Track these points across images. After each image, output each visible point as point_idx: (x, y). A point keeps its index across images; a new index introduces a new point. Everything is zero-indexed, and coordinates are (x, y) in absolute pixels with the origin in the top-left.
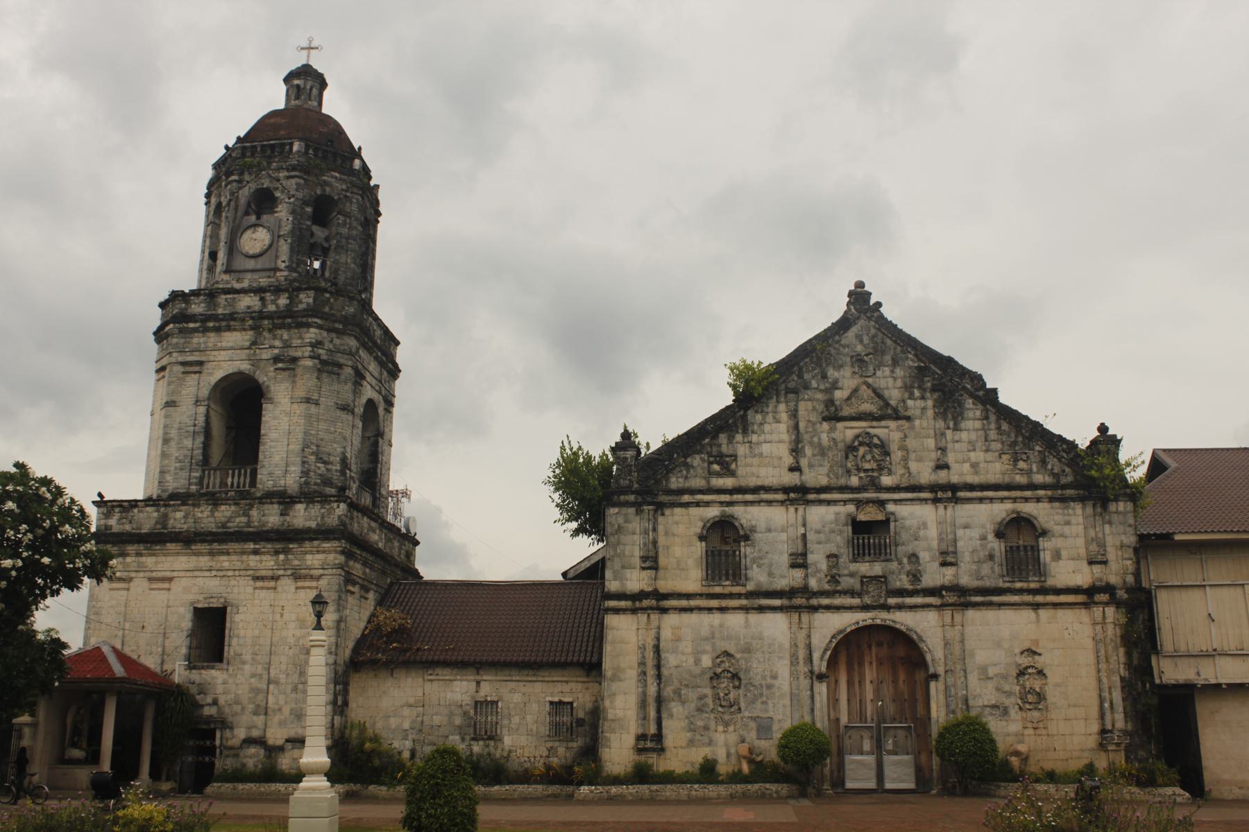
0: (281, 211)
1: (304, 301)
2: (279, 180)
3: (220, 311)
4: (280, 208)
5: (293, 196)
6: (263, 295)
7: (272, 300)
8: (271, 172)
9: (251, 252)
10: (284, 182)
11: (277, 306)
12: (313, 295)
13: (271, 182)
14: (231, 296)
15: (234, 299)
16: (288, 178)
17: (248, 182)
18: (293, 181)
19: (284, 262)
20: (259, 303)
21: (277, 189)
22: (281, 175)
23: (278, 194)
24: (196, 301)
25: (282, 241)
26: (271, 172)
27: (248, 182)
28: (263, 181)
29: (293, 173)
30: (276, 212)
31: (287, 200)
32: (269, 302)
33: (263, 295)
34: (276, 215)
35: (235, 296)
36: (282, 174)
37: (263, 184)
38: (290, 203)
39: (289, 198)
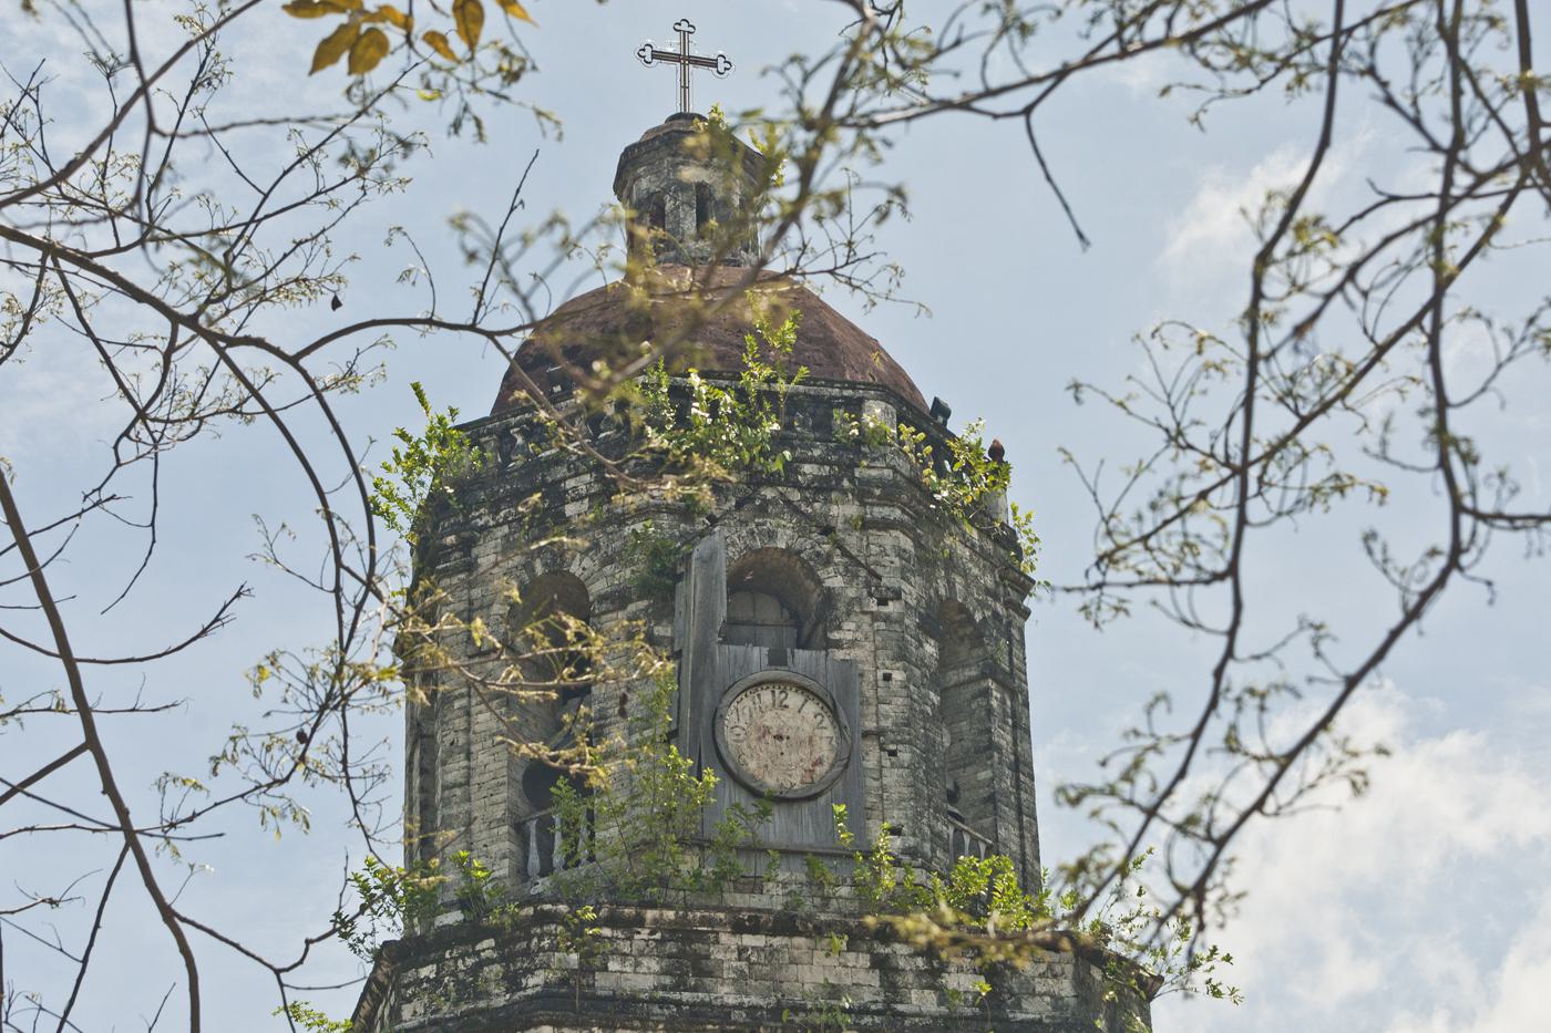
0: (853, 643)
1: (1040, 988)
2: (827, 530)
3: (726, 994)
4: (847, 631)
5: (897, 595)
6: (882, 950)
7: (919, 973)
8: (795, 496)
9: (771, 782)
10: (852, 541)
11: (944, 996)
12: (1069, 969)
13: (803, 532)
14: (757, 941)
15: (772, 952)
16: (866, 525)
17: (713, 520)
18: (891, 539)
19: (895, 831)
20: (874, 979)
21: (827, 561)
22: (835, 510)
23: (835, 581)
24: (625, 947)
25: (872, 757)
26: (795, 496)
27: (713, 520)
28: (770, 523)
29: (879, 512)
30: (838, 645)
31: (873, 607)
32: (910, 978)
33: (882, 950)
34: (840, 654)
35: (777, 941)
36: (843, 510)
37: (772, 535)
38: (887, 619)
39: (883, 602)
